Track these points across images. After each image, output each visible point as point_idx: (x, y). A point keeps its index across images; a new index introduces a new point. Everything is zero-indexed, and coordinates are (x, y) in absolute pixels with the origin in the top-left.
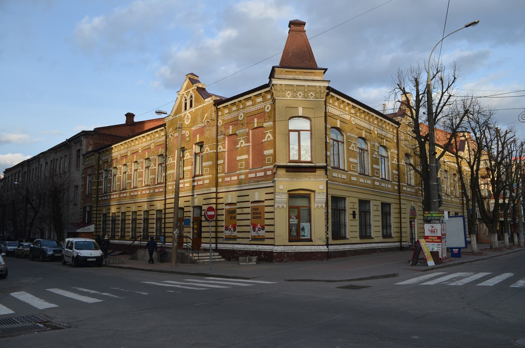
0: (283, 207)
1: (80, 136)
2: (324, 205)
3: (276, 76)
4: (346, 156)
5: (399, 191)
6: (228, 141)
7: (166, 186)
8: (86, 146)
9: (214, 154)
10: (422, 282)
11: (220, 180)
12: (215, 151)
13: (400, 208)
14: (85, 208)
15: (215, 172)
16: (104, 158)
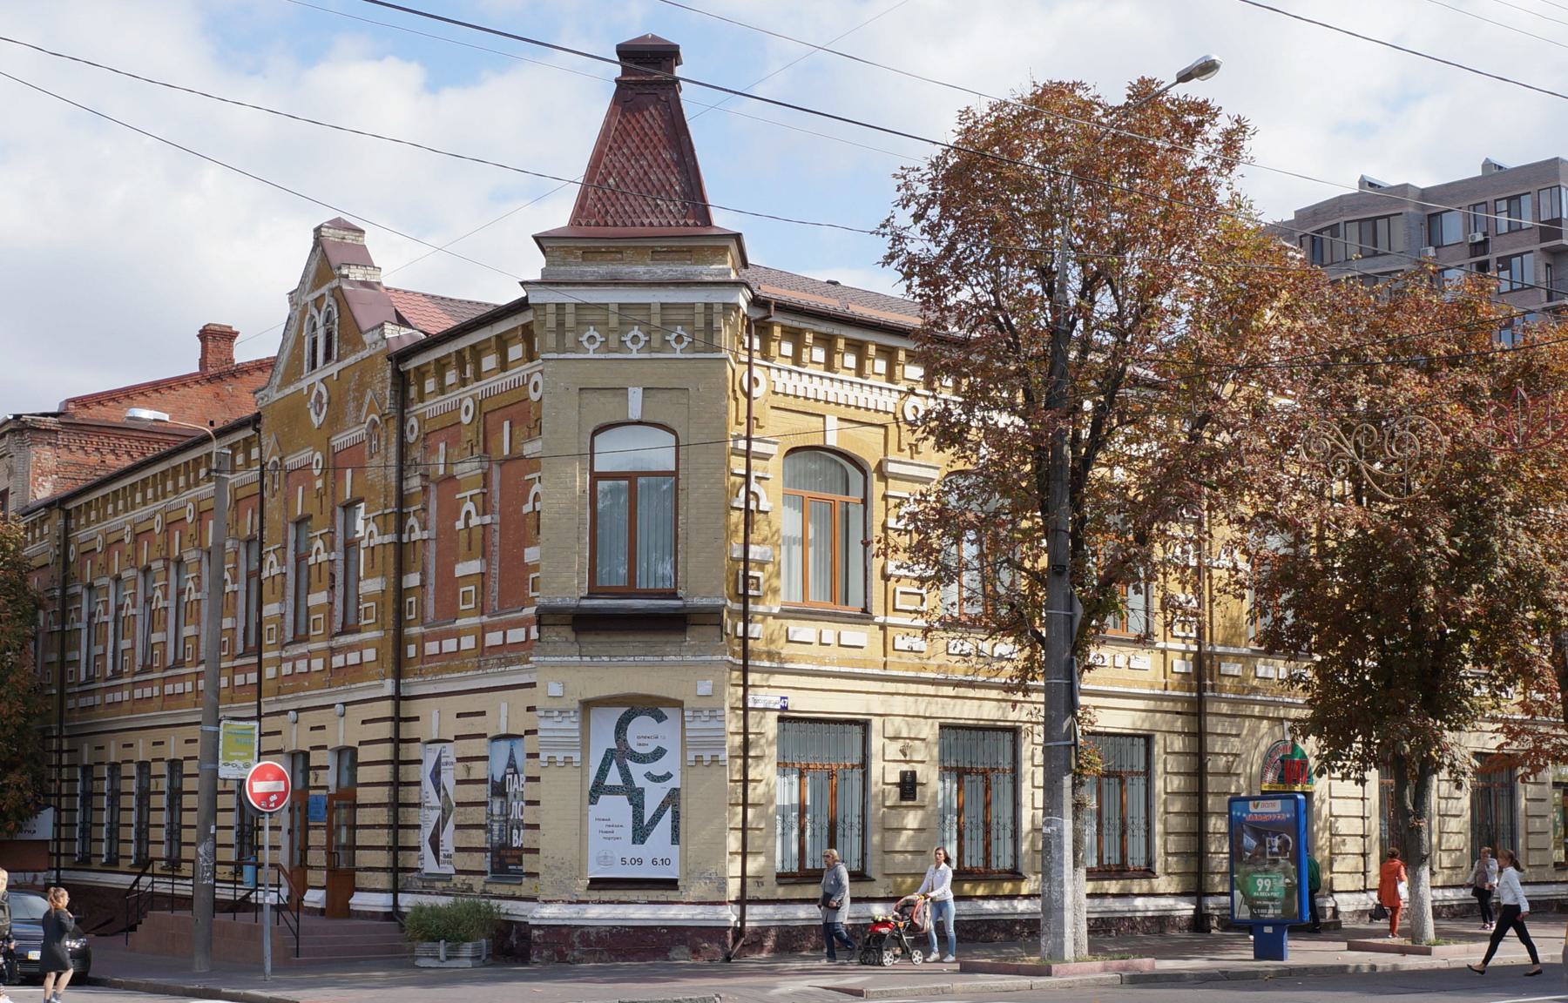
0: (568, 761)
6: (438, 498)
9: (391, 551)
11: (412, 651)
15: (390, 618)
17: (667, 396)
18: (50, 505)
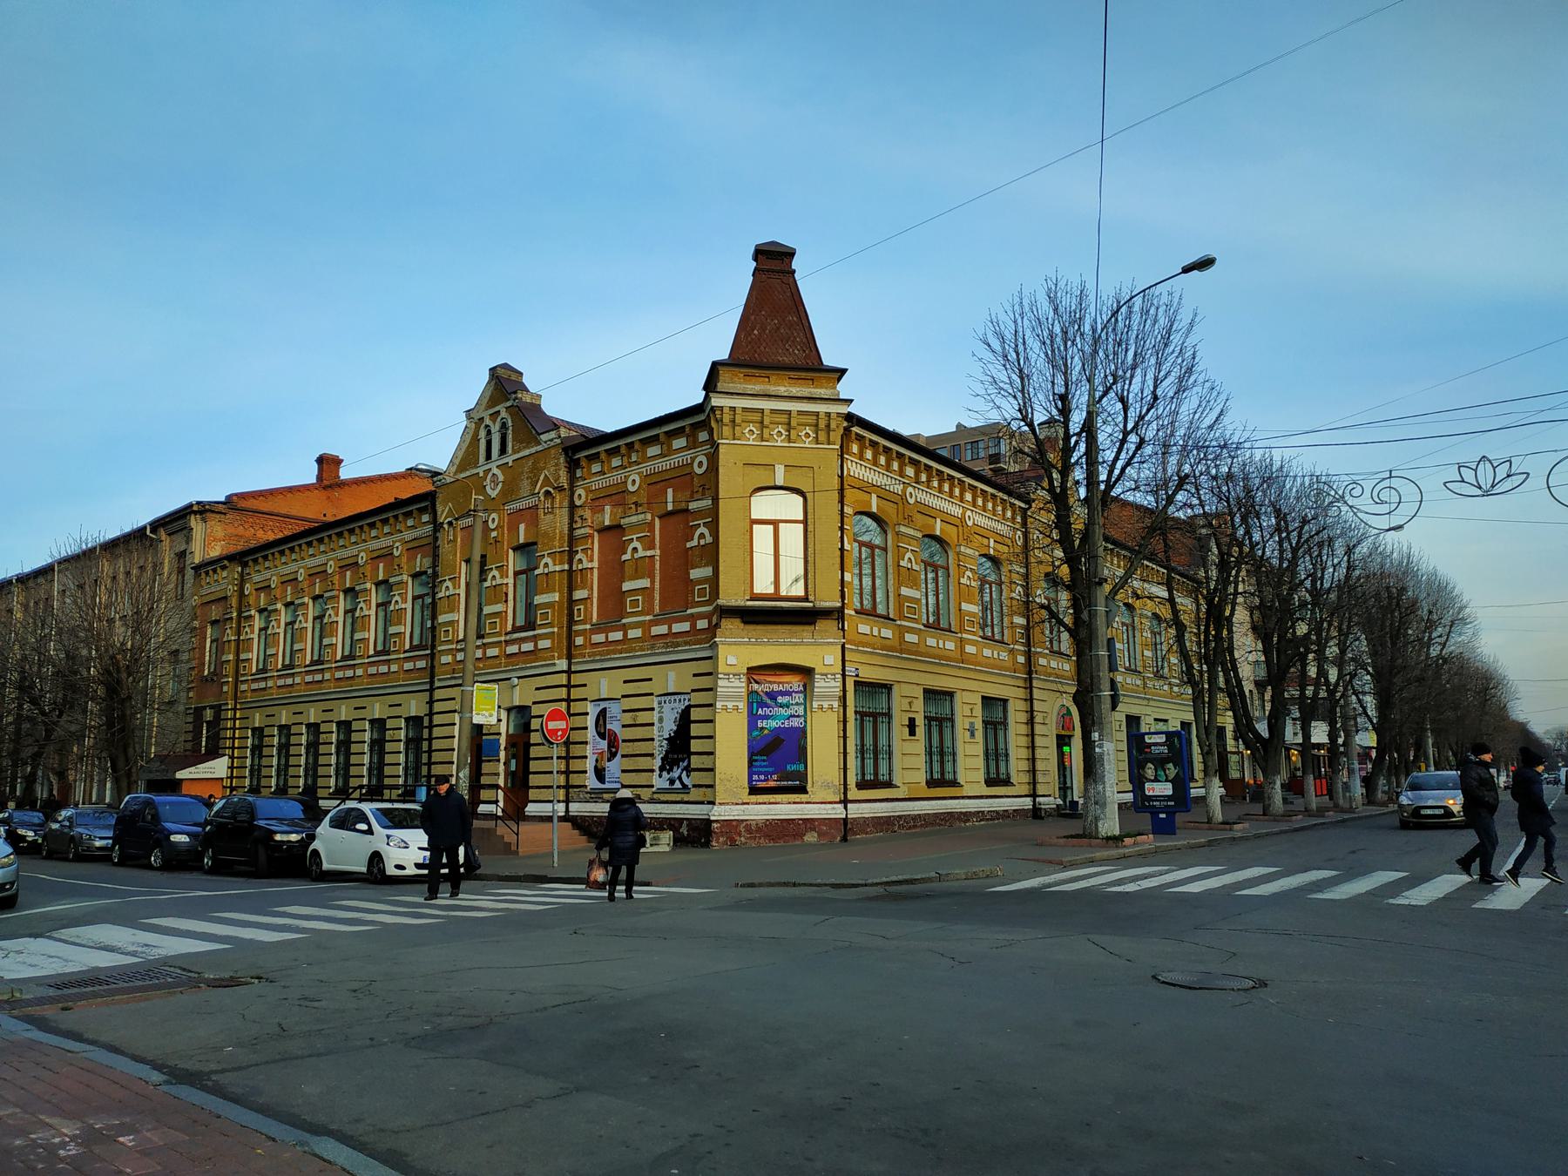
1: (184, 516)
2: (836, 704)
3: (720, 387)
4: (891, 582)
5: (1030, 668)
7: (432, 656)
8: (207, 542)
9: (565, 575)
10: (1050, 885)
11: (579, 641)
12: (566, 567)
13: (1032, 711)
14: (199, 712)
16: (257, 578)
17: (799, 471)
18: (231, 558)
